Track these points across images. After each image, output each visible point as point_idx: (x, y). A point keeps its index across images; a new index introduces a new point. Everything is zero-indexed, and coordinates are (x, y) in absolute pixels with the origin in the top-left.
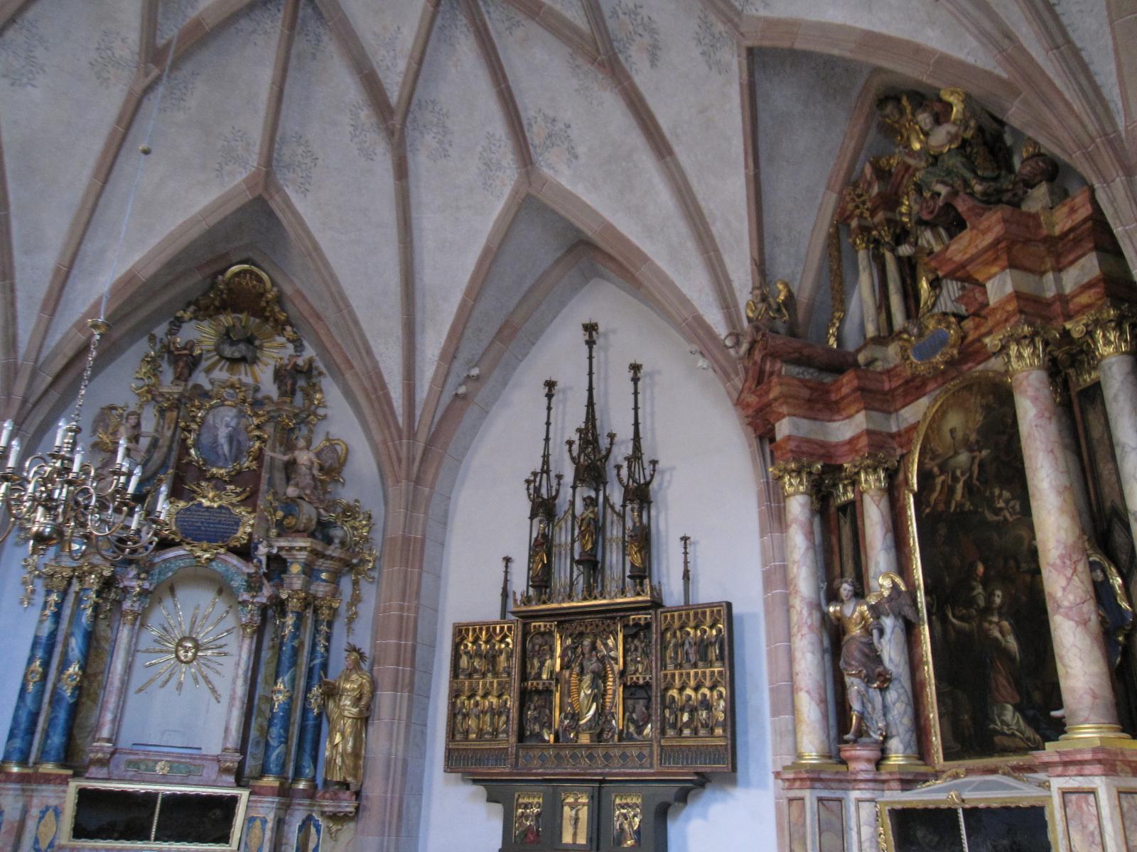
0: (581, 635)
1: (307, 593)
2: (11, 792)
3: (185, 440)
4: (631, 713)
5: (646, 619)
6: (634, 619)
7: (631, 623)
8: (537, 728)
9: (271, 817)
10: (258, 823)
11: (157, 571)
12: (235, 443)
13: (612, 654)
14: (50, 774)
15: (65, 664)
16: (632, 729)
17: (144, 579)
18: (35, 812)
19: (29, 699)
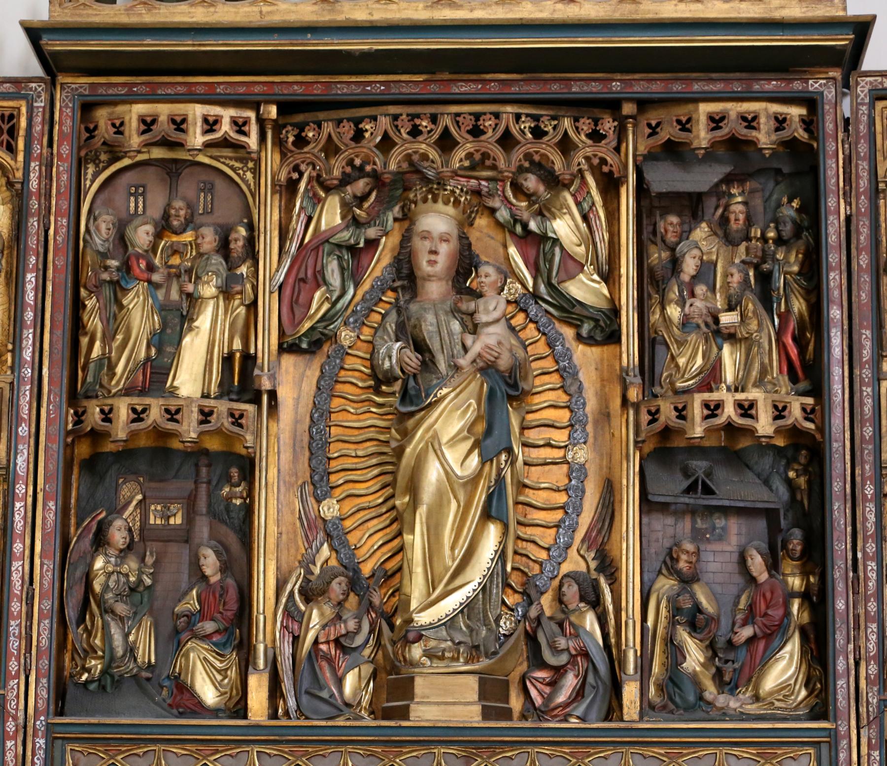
0: (400, 191)
4: (687, 580)
5: (781, 122)
6: (716, 121)
7: (702, 136)
8: (146, 649)
13: (586, 288)
16: (694, 656)
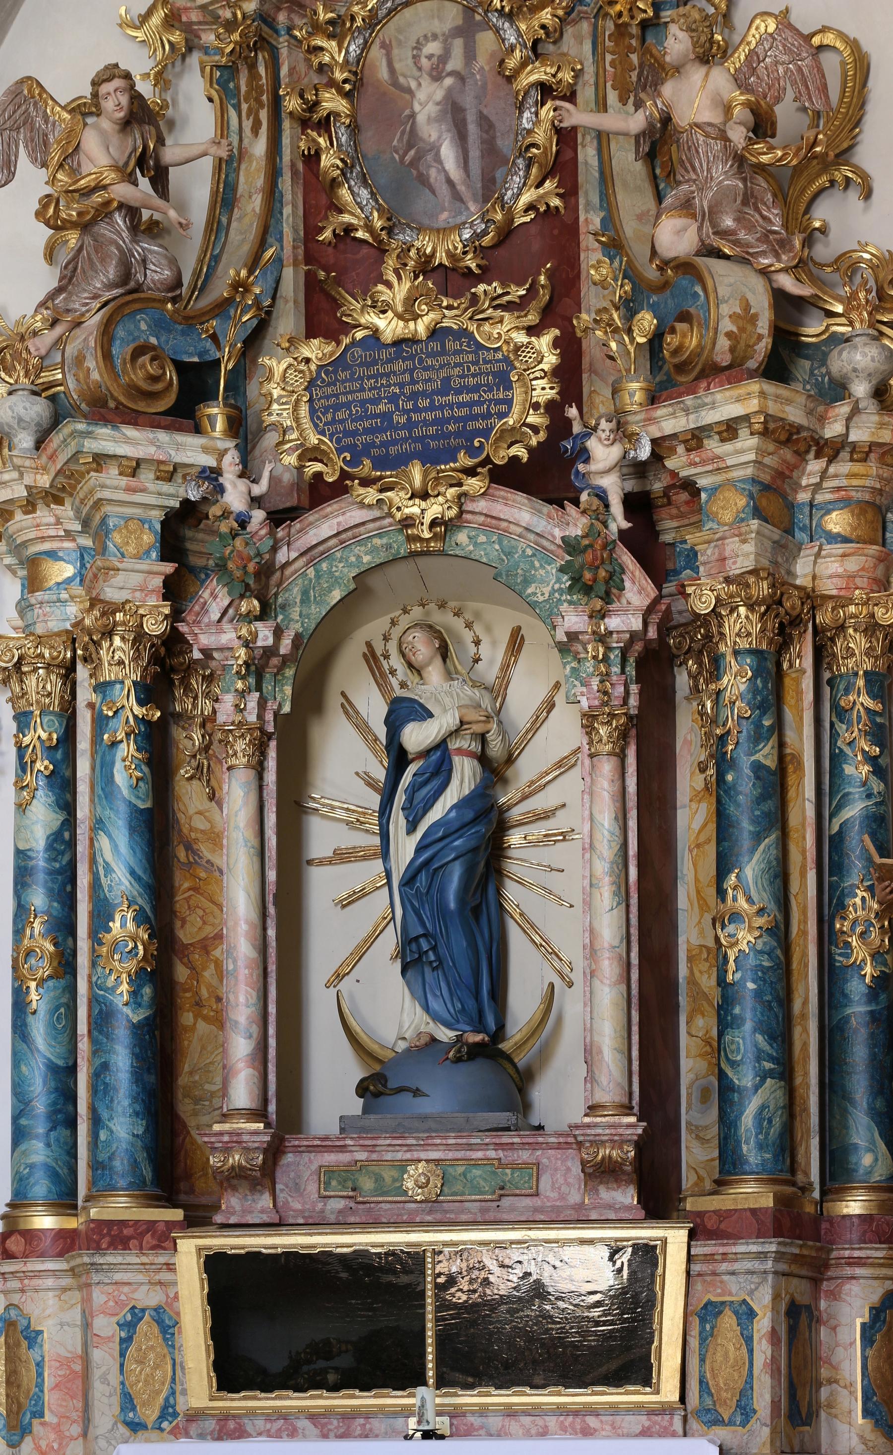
1: (781, 583)
2: (50, 1282)
3: (312, 158)
9: (762, 1300)
10: (728, 1321)
11: (296, 592)
12: (472, 129)
14: (123, 1223)
15: (102, 915)
17: (249, 618)
18: (106, 1326)
19: (38, 1029)
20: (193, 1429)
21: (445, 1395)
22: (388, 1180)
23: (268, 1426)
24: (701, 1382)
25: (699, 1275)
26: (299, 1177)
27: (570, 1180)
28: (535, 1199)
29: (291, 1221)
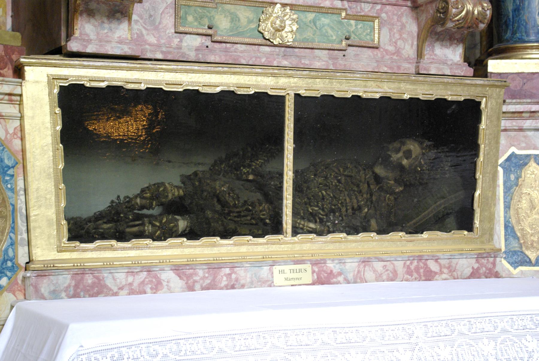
20: (45, 286)
21: (301, 242)
22: (244, 21)
23: (130, 279)
24: (506, 227)
25: (505, 130)
26: (154, 9)
27: (404, 36)
28: (376, 51)
29: (149, 56)
